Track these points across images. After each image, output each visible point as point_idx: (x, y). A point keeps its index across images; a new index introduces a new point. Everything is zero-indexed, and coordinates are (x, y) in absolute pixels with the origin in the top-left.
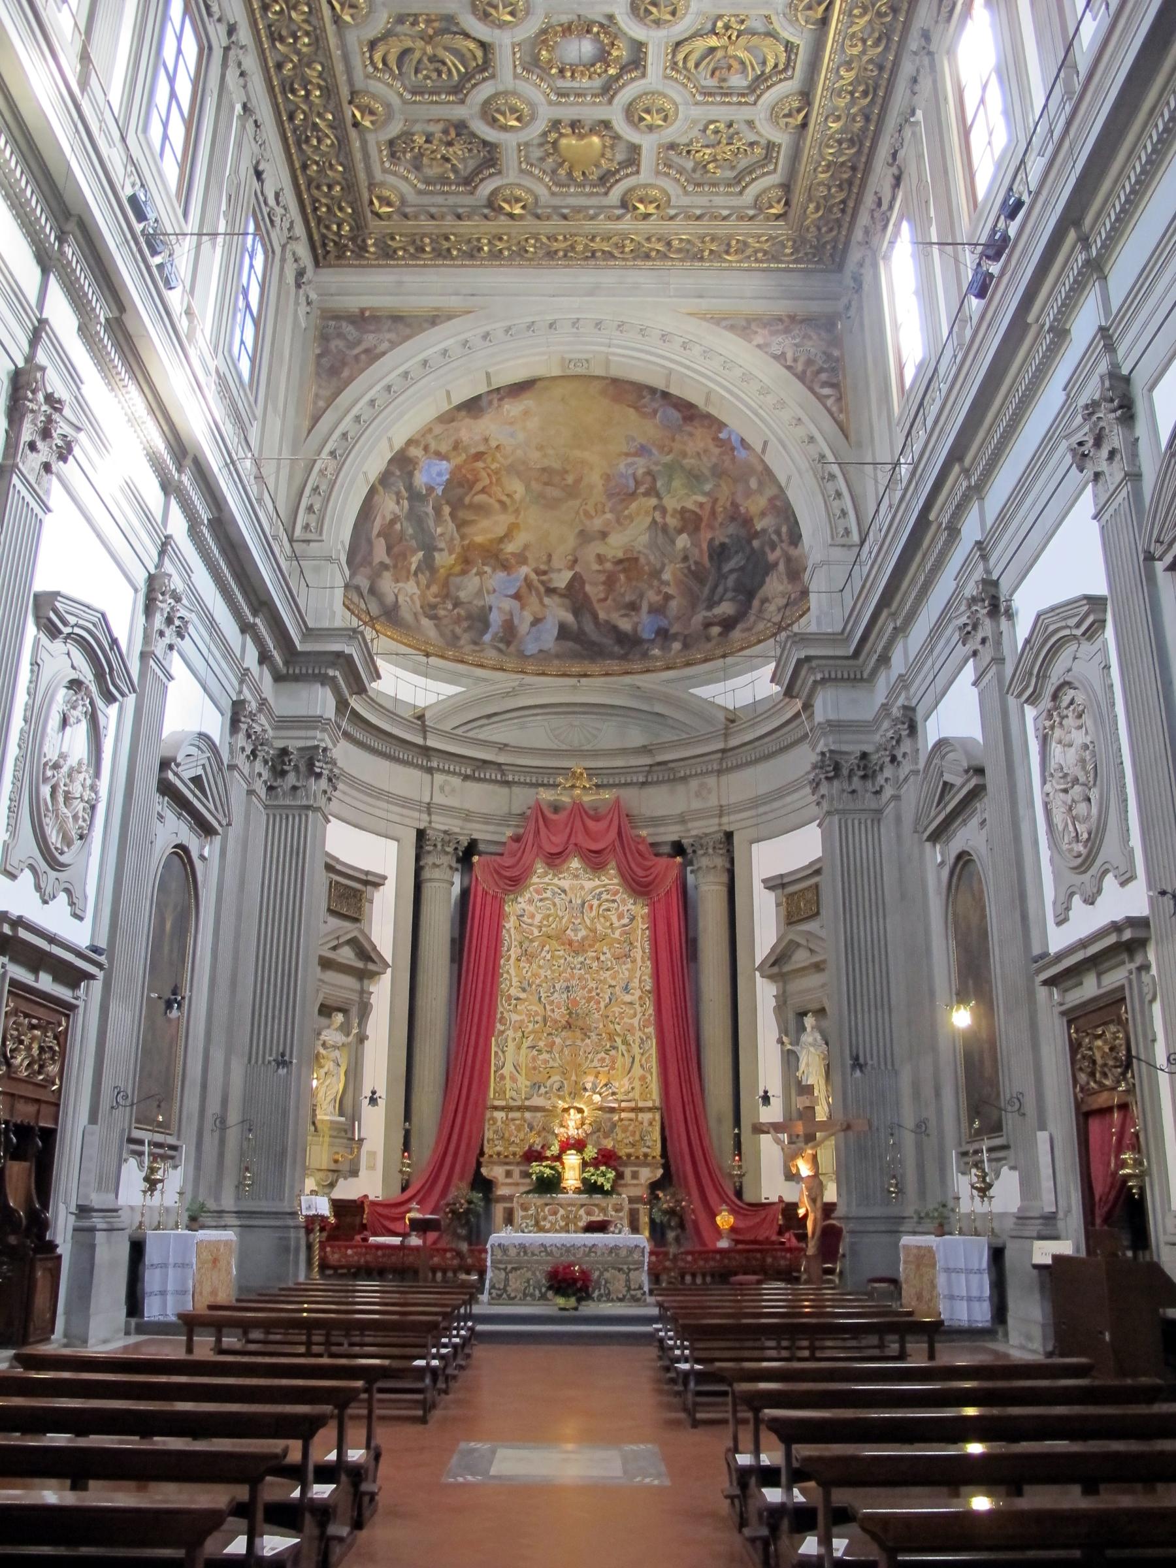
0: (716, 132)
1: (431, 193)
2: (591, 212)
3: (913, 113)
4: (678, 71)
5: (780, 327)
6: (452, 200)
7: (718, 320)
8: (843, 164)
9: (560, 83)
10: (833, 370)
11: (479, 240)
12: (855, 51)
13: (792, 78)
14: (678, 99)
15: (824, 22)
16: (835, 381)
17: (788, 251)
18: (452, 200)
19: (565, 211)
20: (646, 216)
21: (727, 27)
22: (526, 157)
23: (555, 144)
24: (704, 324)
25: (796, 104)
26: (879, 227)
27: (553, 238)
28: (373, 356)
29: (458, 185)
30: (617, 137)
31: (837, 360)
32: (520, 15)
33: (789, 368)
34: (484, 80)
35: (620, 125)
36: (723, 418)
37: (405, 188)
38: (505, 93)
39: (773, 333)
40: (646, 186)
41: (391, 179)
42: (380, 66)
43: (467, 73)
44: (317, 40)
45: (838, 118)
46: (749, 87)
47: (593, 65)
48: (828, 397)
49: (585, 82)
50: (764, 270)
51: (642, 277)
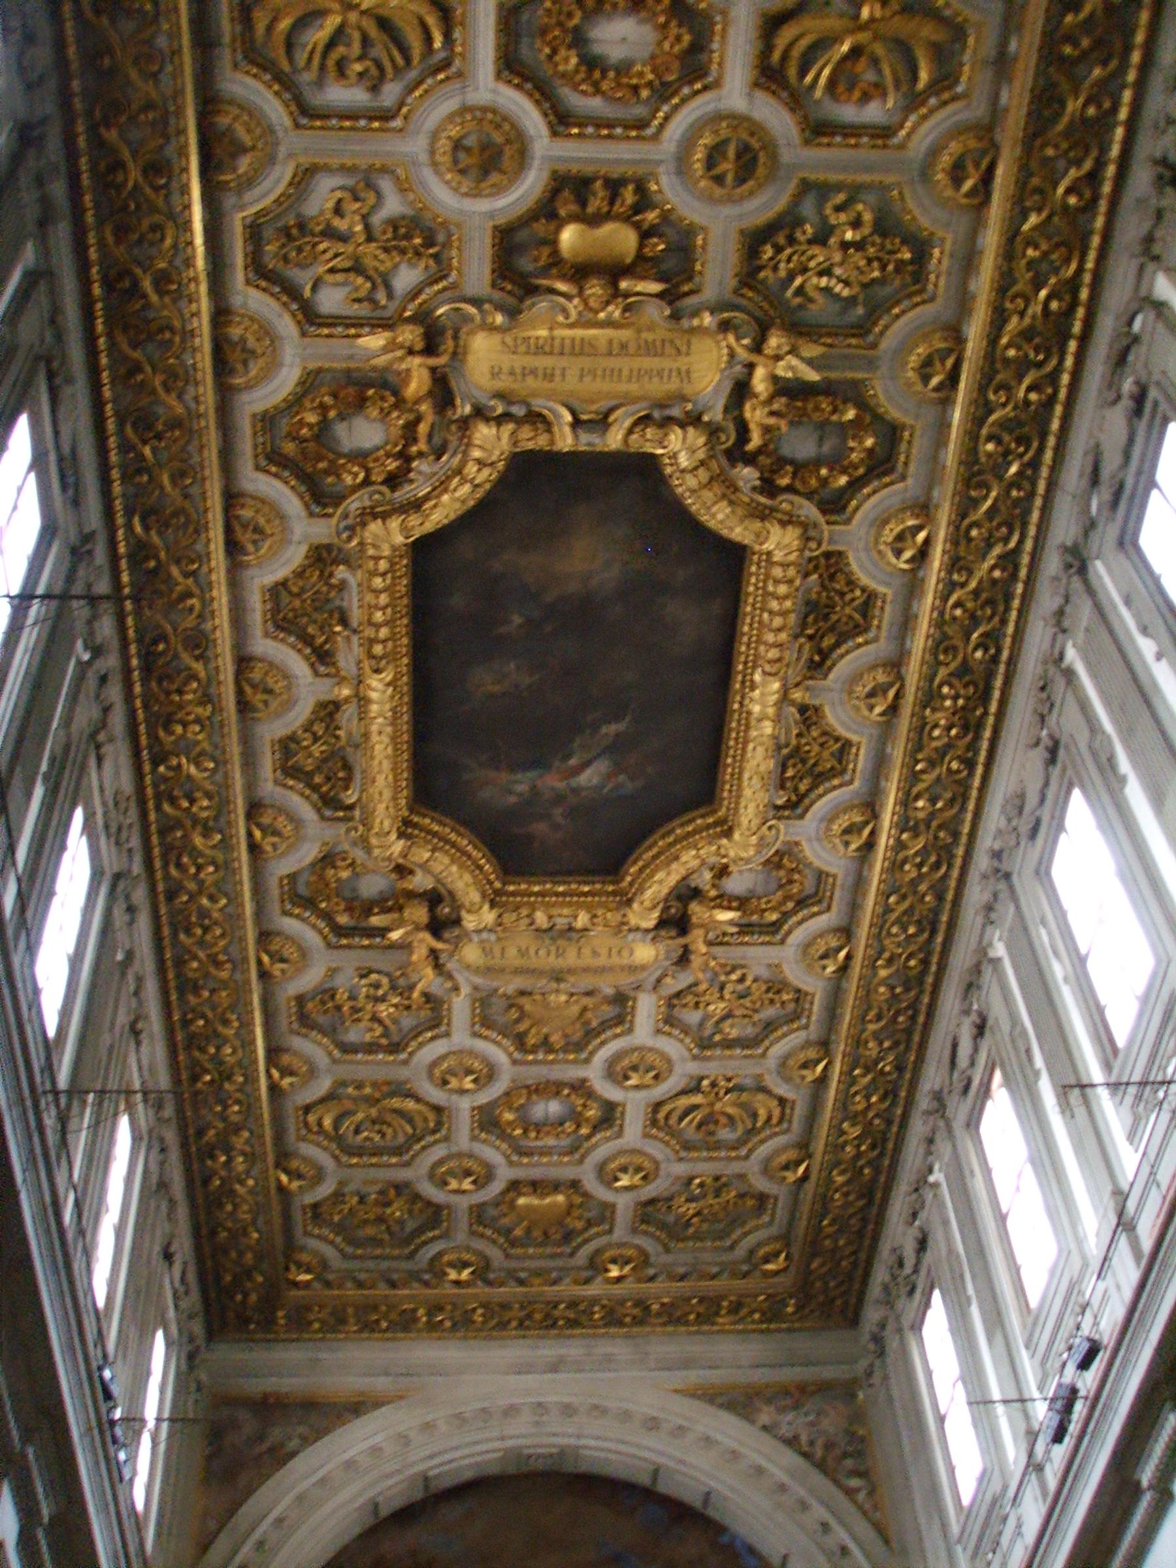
0: (701, 1185)
1: (360, 1257)
2: (554, 1275)
3: (930, 1171)
4: (659, 1129)
5: (788, 1401)
6: (385, 1265)
7: (712, 1396)
8: (851, 1216)
9: (525, 1143)
10: (859, 1454)
11: (414, 1310)
12: (860, 1107)
13: (788, 1130)
14: (659, 1156)
15: (823, 1080)
16: (862, 1468)
17: (790, 1310)
18: (385, 1265)
19: (523, 1275)
20: (619, 1279)
21: (713, 1085)
22: (479, 1216)
23: (512, 1204)
24: (697, 1403)
25: (792, 1155)
26: (904, 1291)
27: (505, 1306)
28: (280, 1457)
29: (392, 1247)
30: (586, 1195)
31: (863, 1440)
32: (482, 1081)
33: (805, 1455)
34: (435, 1142)
35: (591, 1184)
36: (727, 1521)
37: (329, 1252)
38: (460, 1155)
39: (781, 1410)
40: (623, 1245)
41: (313, 1243)
42: (315, 1129)
43: (414, 1135)
44: (249, 1105)
45: (842, 1173)
46: (738, 1140)
47: (561, 1124)
48: (858, 1490)
49: (550, 1141)
50: (762, 1331)
51: (617, 1347)
